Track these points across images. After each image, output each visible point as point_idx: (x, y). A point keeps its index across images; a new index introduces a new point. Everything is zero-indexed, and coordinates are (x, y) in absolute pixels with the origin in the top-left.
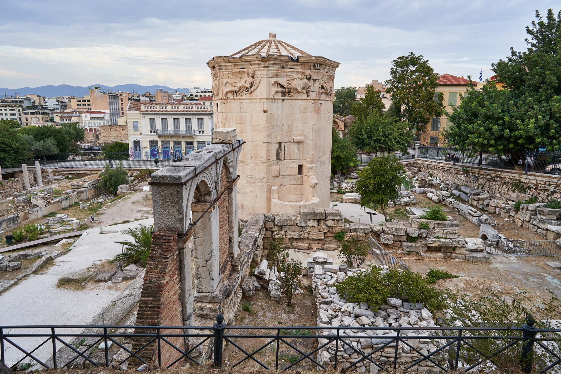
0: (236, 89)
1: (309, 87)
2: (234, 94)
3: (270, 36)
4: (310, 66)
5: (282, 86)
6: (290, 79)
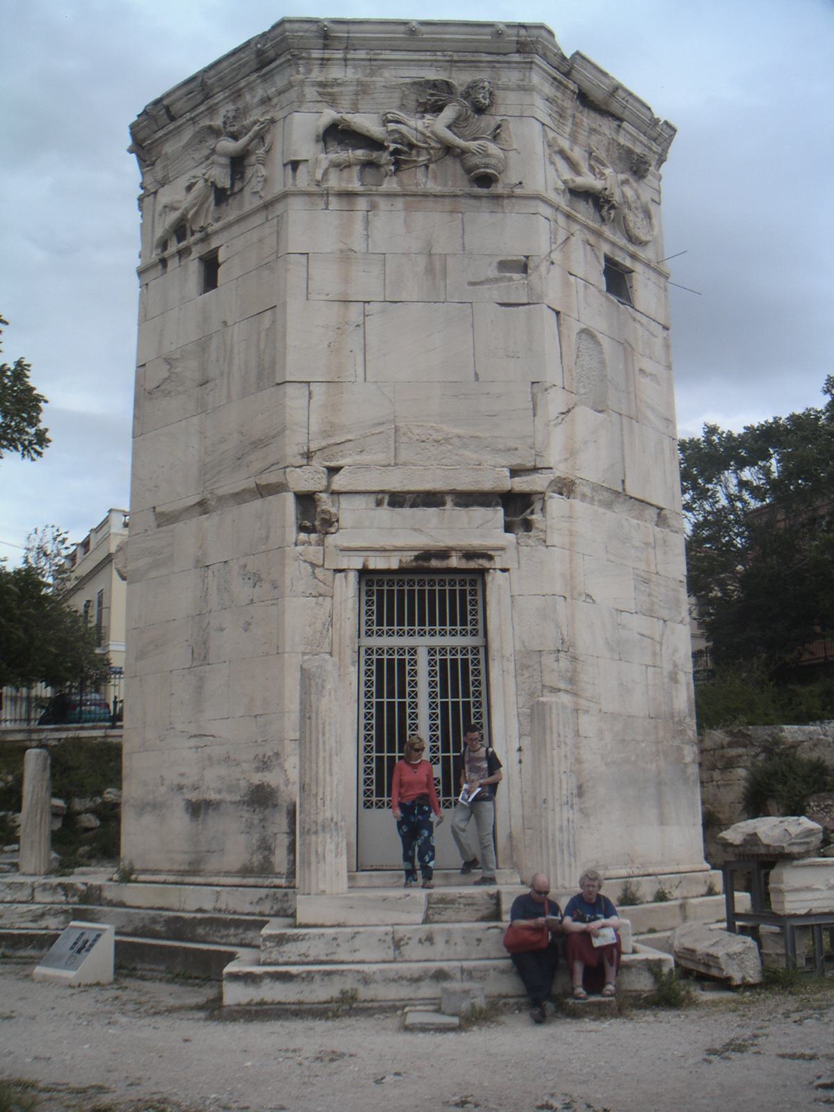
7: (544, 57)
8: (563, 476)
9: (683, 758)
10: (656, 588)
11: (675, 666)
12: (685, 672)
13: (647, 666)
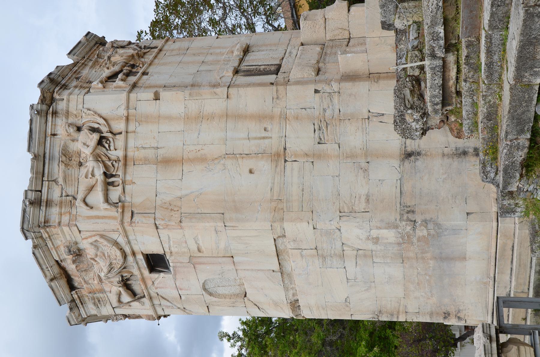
0: (99, 172)
2: (112, 184)
7: (80, 315)
8: (291, 311)
9: (424, 236)
10: (326, 251)
11: (368, 238)
12: (371, 230)
13: (374, 262)
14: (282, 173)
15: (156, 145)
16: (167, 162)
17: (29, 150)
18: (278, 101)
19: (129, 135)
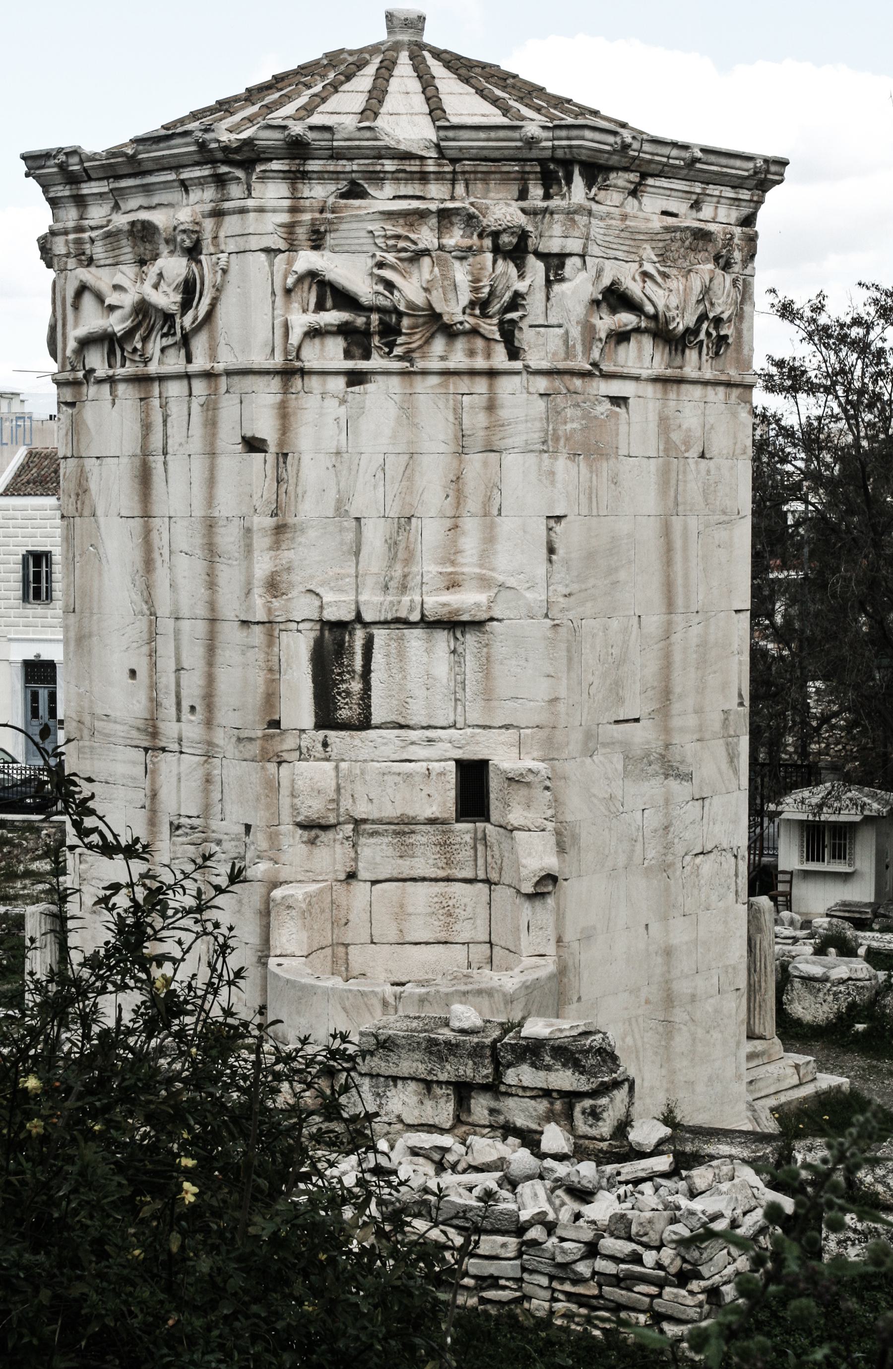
0: (117, 324)
1: (516, 301)
3: (391, 29)
4: (523, 179)
5: (345, 299)
6: (390, 258)
14: (129, 742)
15: (170, 450)
16: (144, 478)
17: (138, 141)
18: (234, 739)
19: (185, 382)
